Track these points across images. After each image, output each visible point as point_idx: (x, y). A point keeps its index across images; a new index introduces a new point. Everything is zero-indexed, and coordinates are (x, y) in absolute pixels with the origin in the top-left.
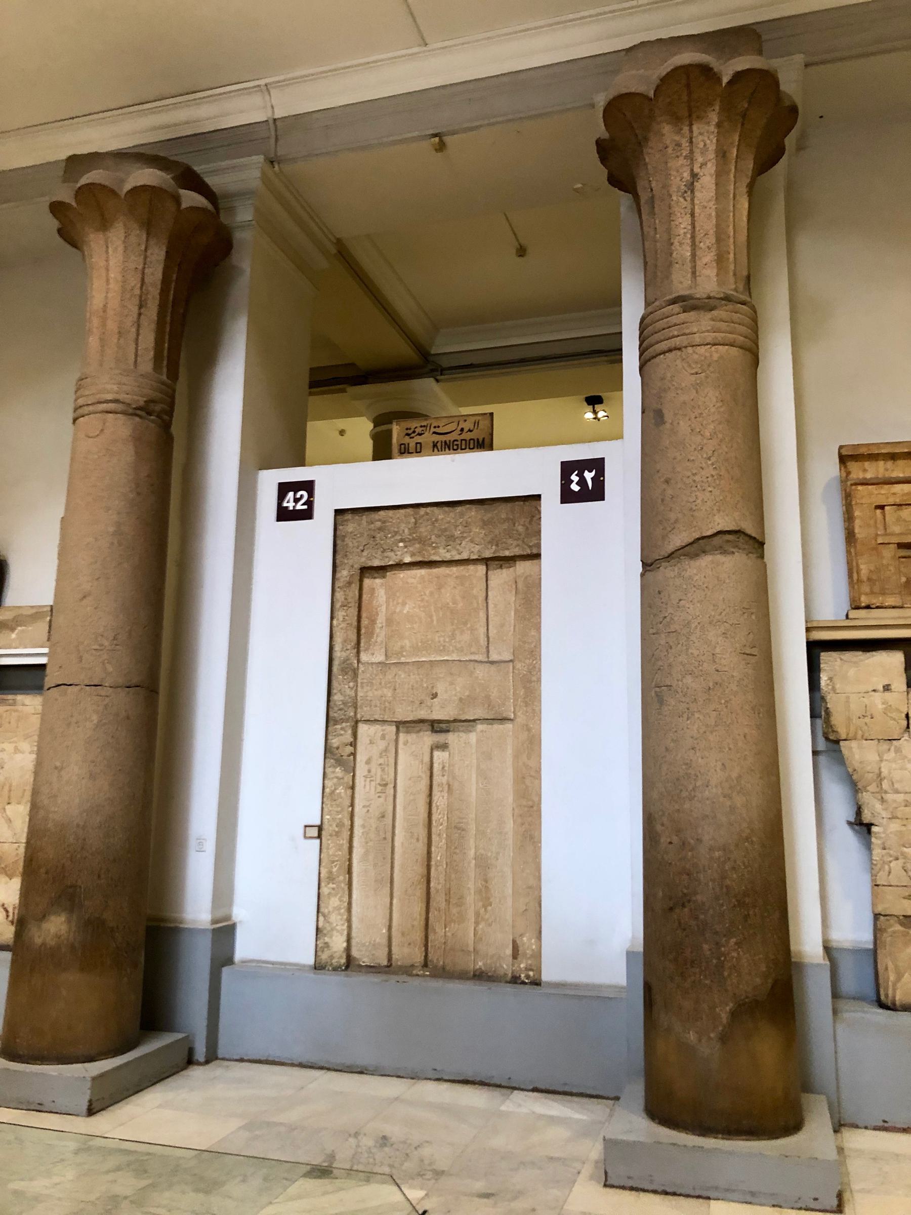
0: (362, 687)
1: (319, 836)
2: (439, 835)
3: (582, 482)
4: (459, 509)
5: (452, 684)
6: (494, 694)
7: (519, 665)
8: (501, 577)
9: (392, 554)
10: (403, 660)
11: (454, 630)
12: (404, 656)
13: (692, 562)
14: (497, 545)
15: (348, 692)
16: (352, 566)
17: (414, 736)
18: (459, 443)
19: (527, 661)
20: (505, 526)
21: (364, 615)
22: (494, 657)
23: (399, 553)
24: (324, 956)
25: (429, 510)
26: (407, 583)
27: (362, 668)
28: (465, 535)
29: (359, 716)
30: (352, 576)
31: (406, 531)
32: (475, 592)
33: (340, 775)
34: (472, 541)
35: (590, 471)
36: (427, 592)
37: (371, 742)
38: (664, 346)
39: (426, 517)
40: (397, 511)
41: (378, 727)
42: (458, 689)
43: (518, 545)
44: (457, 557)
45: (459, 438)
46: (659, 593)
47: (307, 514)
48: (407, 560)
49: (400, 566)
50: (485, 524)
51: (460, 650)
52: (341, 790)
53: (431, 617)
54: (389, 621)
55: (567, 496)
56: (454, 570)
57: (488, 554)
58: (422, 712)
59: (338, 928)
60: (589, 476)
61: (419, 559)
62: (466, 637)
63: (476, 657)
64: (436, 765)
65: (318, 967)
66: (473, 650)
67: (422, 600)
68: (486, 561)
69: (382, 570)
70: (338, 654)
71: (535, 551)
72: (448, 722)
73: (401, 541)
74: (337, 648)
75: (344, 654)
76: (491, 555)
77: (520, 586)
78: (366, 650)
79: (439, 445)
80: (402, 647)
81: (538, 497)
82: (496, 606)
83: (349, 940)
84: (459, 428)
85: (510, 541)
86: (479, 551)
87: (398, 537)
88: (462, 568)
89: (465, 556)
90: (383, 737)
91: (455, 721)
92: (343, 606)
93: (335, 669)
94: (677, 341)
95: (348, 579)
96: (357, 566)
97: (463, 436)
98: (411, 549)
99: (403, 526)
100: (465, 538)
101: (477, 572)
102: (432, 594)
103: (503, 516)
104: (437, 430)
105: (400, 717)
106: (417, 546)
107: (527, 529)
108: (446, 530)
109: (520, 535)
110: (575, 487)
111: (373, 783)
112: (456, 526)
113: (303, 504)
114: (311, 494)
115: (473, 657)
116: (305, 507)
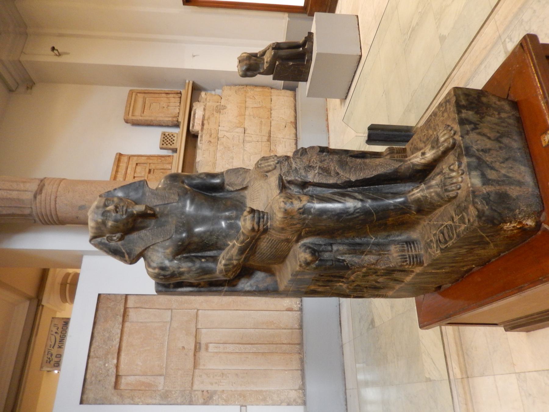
0: (175, 388)
1: (246, 406)
4: (95, 334)
7: (174, 306)
8: (132, 314)
9: (111, 370)
10: (164, 366)
14: (117, 315)
15: (177, 394)
16: (113, 394)
20: (109, 311)
21: (139, 388)
22: (169, 319)
24: (300, 401)
25: (92, 350)
27: (166, 388)
29: (189, 389)
30: (118, 394)
31: (101, 362)
33: (217, 397)
37: (202, 383)
38: (53, 203)
39: (96, 352)
40: (89, 368)
41: (196, 379)
44: (119, 335)
45: (60, 334)
48: (115, 361)
49: (117, 366)
52: (224, 396)
54: (145, 374)
56: (125, 338)
57: (120, 319)
59: (286, 394)
61: (116, 355)
63: (168, 327)
64: (215, 351)
65: (304, 403)
67: (137, 354)
69: (117, 376)
70: (157, 401)
71: (124, 297)
72: (196, 342)
73: (104, 365)
74: (154, 401)
75: (158, 398)
77: (138, 306)
78: (157, 386)
79: (60, 345)
81: (99, 295)
83: (292, 390)
84: (55, 334)
85: (117, 309)
87: (102, 367)
89: (119, 331)
90: (201, 376)
91: (196, 337)
92: (133, 399)
93: (165, 403)
94: (53, 197)
95: (119, 397)
96: (113, 391)
99: (97, 365)
103: (104, 312)
104: (52, 346)
106: (109, 356)
108: (104, 341)
111: (222, 381)
112: (104, 336)
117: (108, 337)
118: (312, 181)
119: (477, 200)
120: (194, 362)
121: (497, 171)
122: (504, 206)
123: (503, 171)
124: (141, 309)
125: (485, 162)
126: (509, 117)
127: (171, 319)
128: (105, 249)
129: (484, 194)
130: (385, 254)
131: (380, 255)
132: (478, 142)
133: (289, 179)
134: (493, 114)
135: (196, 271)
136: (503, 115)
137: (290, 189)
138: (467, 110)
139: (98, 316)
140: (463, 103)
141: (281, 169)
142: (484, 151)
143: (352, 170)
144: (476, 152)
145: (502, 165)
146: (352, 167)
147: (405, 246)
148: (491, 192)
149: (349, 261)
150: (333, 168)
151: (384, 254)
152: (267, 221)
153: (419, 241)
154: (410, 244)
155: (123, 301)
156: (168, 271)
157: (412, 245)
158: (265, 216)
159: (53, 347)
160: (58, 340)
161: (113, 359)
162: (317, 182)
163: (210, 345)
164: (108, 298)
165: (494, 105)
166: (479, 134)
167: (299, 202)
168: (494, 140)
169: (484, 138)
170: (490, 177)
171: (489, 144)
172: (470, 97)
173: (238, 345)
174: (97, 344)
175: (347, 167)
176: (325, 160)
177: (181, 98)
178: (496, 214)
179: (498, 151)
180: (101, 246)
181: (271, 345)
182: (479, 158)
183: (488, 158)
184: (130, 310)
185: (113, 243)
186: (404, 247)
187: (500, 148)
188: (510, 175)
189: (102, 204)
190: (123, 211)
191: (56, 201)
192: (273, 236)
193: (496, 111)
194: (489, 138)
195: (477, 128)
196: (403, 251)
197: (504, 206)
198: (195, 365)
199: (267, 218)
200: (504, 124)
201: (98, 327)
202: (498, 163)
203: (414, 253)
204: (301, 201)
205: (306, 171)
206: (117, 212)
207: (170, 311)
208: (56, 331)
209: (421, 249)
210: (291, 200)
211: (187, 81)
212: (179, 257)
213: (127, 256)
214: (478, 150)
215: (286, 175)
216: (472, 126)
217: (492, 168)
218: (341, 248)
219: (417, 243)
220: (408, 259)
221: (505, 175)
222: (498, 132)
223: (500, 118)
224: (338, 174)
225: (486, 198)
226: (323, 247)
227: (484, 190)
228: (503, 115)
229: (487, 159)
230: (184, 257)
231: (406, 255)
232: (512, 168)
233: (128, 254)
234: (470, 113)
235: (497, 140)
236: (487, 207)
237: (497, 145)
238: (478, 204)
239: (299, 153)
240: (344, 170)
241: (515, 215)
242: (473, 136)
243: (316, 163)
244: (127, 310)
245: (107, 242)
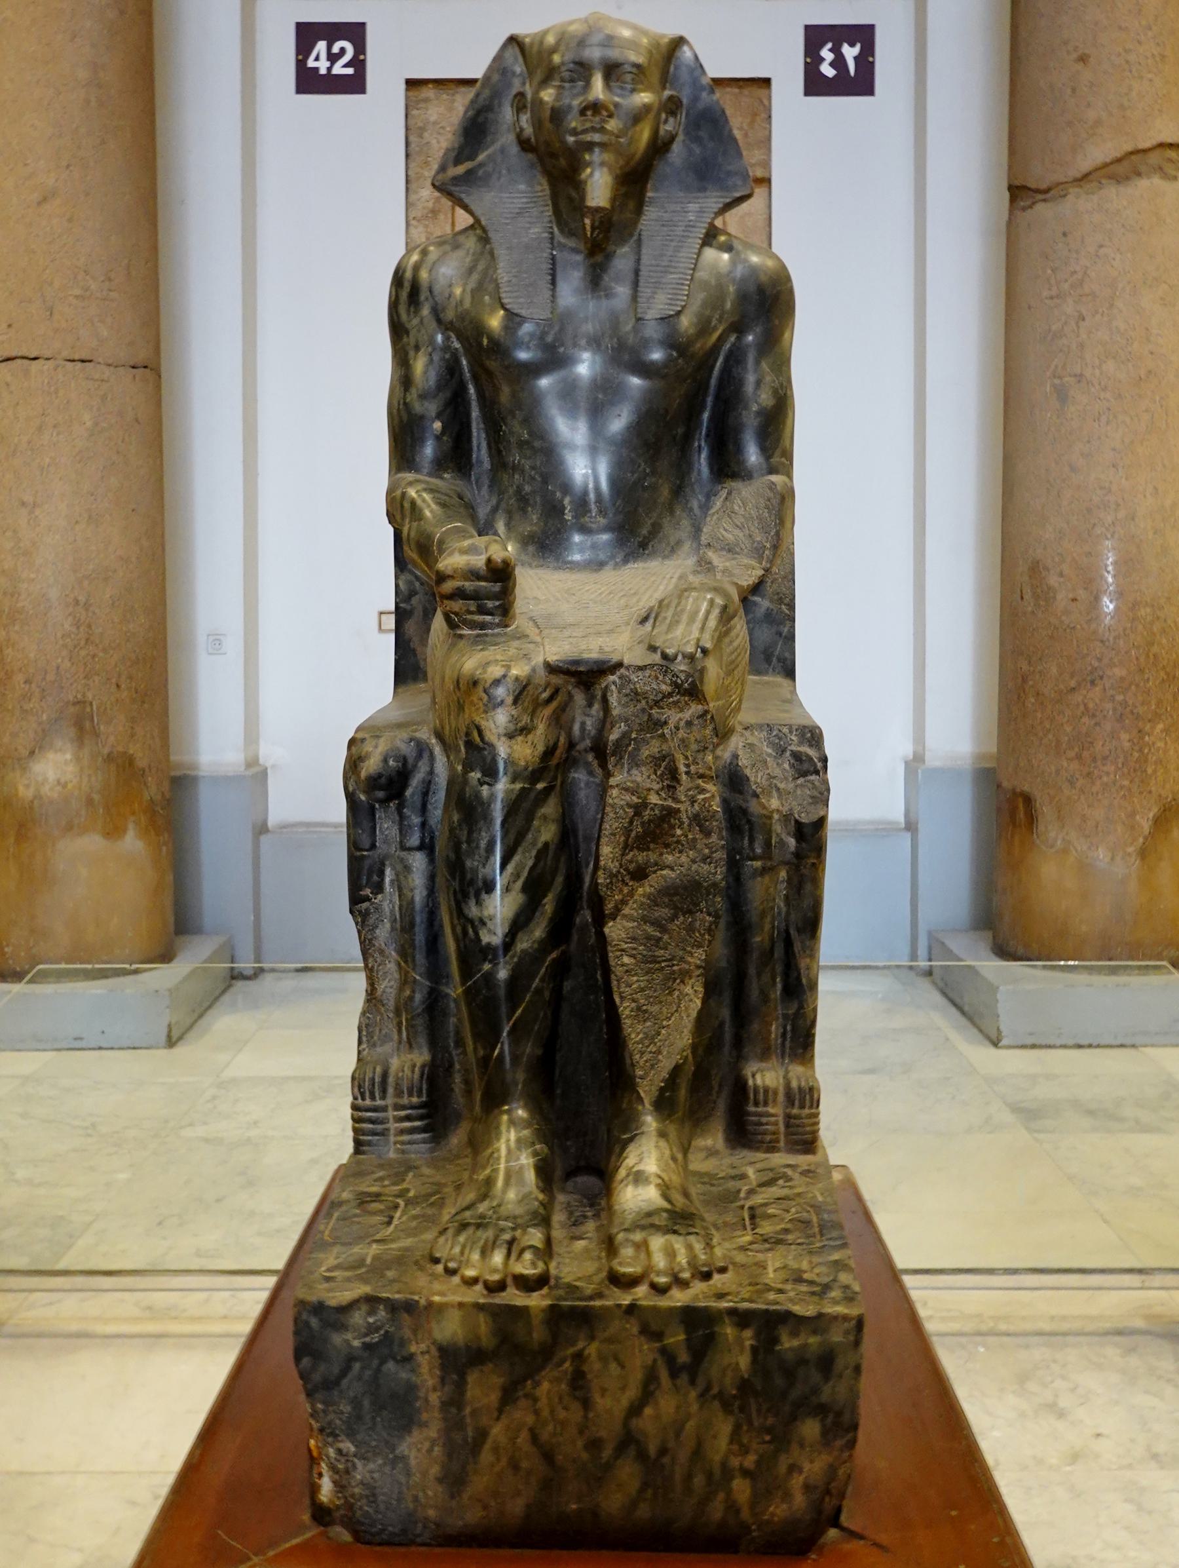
13: (1122, 189)
35: (852, 45)
46: (1065, 234)
47: (355, 84)
113: (346, 66)
114: (360, 48)
116: (350, 71)
122: (366, 1403)
132: (613, 1366)
142: (578, 1382)
152: (473, 625)
158: (488, 618)
170: (472, 1377)
197: (366, 1403)
199: (483, 626)
202: (530, 1419)
214: (579, 1357)
216: (684, 1357)
229: (546, 1385)
237: (608, 1429)
239: (805, 749)
242: (642, 1353)
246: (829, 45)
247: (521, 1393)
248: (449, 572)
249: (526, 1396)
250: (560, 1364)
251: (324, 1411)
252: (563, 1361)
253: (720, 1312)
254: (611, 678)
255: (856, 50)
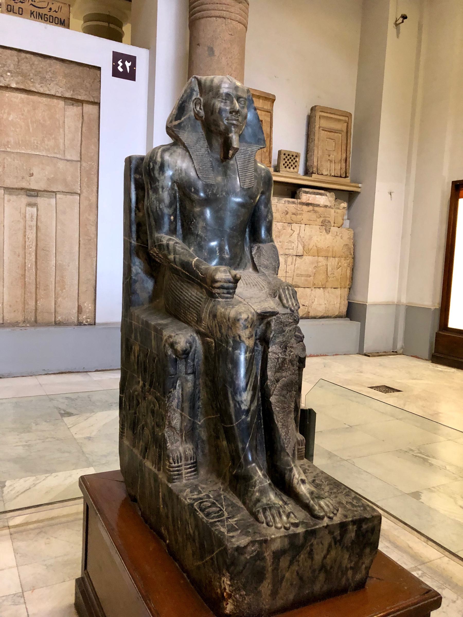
2: (30, 253)
3: (124, 67)
4: (48, 61)
5: (43, 169)
6: (69, 178)
7: (84, 164)
10: (8, 150)
11: (44, 137)
12: (9, 148)
14: (73, 91)
17: (15, 197)
18: (48, 17)
19: (89, 163)
20: (79, 80)
22: (68, 157)
23: (8, 80)
25: (28, 56)
26: (12, 101)
28: (53, 79)
31: (12, 66)
32: (57, 116)
34: (57, 84)
35: (129, 62)
36: (26, 110)
38: (217, 13)
39: (25, 60)
40: (4, 50)
42: (47, 173)
43: (85, 95)
44: (47, 92)
45: (49, 14)
48: (14, 85)
50: (66, 76)
51: (48, 150)
53: (28, 126)
55: (116, 73)
56: (44, 100)
57: (68, 95)
58: (24, 184)
60: (128, 64)
61: (22, 87)
62: (52, 143)
63: (58, 156)
64: (27, 215)
66: (56, 151)
68: (65, 99)
71: (96, 101)
73: (9, 71)
76: (70, 97)
77: (85, 118)
79: (35, 13)
80: (8, 142)
81: (99, 69)
82: (69, 128)
84: (49, 7)
85: (82, 91)
86: (62, 92)
87: (6, 68)
88: (49, 100)
89: (53, 93)
94: (224, 14)
97: (51, 13)
98: (16, 79)
99: (9, 62)
100: (53, 81)
101: (58, 104)
102: (29, 111)
103: (77, 73)
104: (33, 3)
105: (8, 186)
107: (91, 86)
109: (87, 88)
110: (121, 70)
112: (47, 72)
115: (55, 156)
117: (45, 78)
118: (270, 350)
119: (257, 545)
120: (13, 188)
121: (289, 568)
123: (287, 575)
124: (81, 121)
125: (298, 553)
126: (348, 580)
127: (68, 161)
128: (185, 95)
129: (263, 553)
130: (182, 438)
131: (181, 430)
133: (273, 324)
134: (351, 562)
135: (159, 208)
136: (350, 573)
137: (260, 325)
138: (356, 531)
139: (72, 65)
140: (364, 527)
141: (284, 314)
143: (281, 397)
144: (309, 544)
145: (295, 573)
146: (285, 398)
147: (192, 461)
148: (265, 562)
149: (174, 395)
150: (284, 374)
151: (182, 436)
152: (223, 298)
153: (197, 478)
154: (194, 467)
155: (92, 100)
156: (159, 174)
157: (193, 469)
158: (229, 295)
159: (31, 4)
160: (41, 11)
161: (17, 83)
162: (269, 357)
163: (35, 209)
164: (95, 79)
165: (361, 561)
166: (330, 546)
167: (247, 336)
168: (322, 562)
169: (325, 552)
171: (318, 558)
172: (370, 534)
173: (34, 244)
174: (36, 63)
175: (285, 392)
176: (293, 365)
177: (341, 177)
178: (241, 568)
179: (310, 568)
180: (189, 91)
181: (34, 286)
182: (303, 546)
183: (302, 556)
184: (80, 108)
185: (192, 106)
186: (191, 460)
187: (314, 571)
188: (284, 584)
189: (240, 94)
190: (232, 120)
191: (220, 17)
192: (205, 304)
193: (354, 564)
194: (325, 557)
195: (335, 544)
196: (186, 459)
198: (9, 190)
199: (227, 298)
200: (340, 574)
201: (58, 65)
203: (184, 472)
204: (249, 338)
205: (281, 343)
206: (231, 113)
207: (79, 160)
208: (53, 10)
209: (188, 480)
210: (249, 326)
211: (360, 185)
212: (176, 188)
213: (177, 123)
214: (312, 545)
215: (277, 320)
216: (339, 538)
217: (291, 563)
218: (190, 385)
219: (195, 475)
220: (176, 465)
221: (283, 577)
222: (331, 567)
223: (347, 569)
224: (278, 381)
225: (259, 556)
226: (192, 363)
227: (268, 553)
228: (350, 573)
229: (302, 556)
230: (175, 193)
231: (181, 462)
232: (292, 584)
233: (179, 124)
234: (353, 535)
235: (323, 567)
236: (248, 557)
238: (252, 547)
240: (282, 388)
241: (239, 590)
243: (290, 355)
244: (80, 104)
245: (194, 98)
246: (121, 60)
247: (295, 561)
248: (219, 280)
249: (296, 561)
250: (306, 549)
251: (237, 583)
252: (307, 547)
253: (349, 522)
254: (274, 317)
255: (130, 64)
